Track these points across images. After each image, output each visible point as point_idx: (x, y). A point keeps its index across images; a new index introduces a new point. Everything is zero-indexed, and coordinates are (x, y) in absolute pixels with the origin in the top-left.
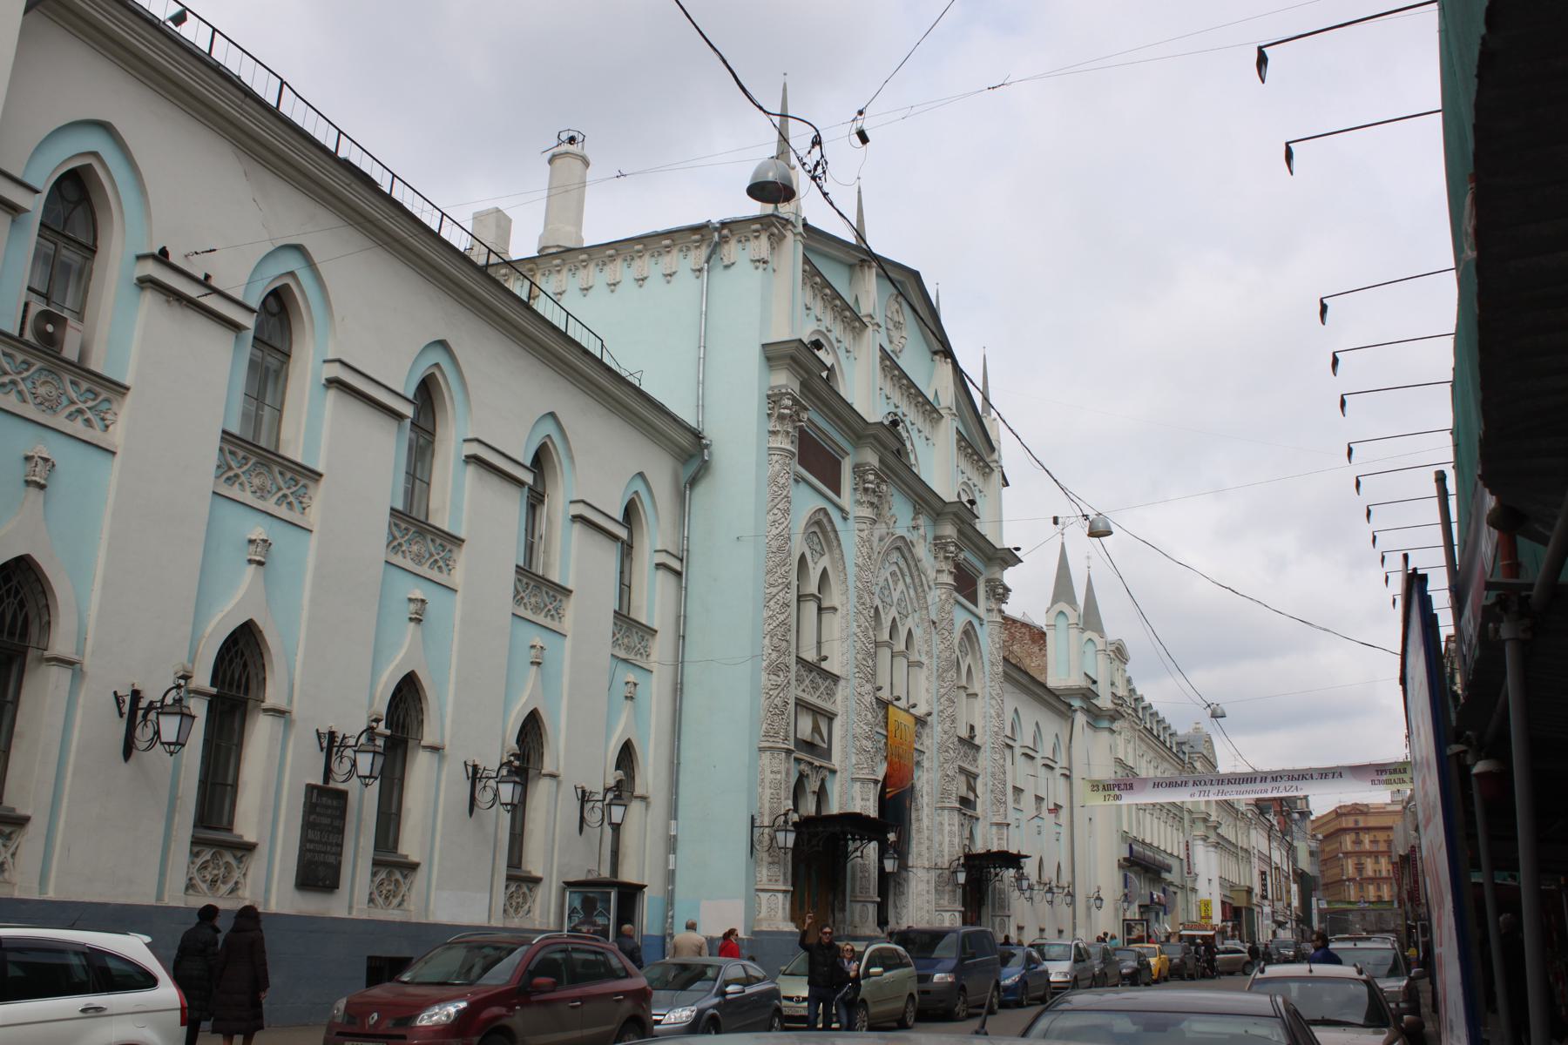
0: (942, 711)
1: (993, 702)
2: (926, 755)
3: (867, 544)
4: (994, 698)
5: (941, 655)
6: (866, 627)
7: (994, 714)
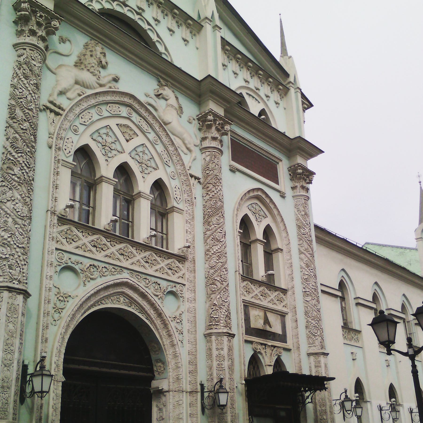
0: (208, 250)
1: (303, 256)
2: (187, 286)
3: (25, 66)
4: (302, 253)
5: (207, 204)
6: (15, 137)
7: (304, 266)
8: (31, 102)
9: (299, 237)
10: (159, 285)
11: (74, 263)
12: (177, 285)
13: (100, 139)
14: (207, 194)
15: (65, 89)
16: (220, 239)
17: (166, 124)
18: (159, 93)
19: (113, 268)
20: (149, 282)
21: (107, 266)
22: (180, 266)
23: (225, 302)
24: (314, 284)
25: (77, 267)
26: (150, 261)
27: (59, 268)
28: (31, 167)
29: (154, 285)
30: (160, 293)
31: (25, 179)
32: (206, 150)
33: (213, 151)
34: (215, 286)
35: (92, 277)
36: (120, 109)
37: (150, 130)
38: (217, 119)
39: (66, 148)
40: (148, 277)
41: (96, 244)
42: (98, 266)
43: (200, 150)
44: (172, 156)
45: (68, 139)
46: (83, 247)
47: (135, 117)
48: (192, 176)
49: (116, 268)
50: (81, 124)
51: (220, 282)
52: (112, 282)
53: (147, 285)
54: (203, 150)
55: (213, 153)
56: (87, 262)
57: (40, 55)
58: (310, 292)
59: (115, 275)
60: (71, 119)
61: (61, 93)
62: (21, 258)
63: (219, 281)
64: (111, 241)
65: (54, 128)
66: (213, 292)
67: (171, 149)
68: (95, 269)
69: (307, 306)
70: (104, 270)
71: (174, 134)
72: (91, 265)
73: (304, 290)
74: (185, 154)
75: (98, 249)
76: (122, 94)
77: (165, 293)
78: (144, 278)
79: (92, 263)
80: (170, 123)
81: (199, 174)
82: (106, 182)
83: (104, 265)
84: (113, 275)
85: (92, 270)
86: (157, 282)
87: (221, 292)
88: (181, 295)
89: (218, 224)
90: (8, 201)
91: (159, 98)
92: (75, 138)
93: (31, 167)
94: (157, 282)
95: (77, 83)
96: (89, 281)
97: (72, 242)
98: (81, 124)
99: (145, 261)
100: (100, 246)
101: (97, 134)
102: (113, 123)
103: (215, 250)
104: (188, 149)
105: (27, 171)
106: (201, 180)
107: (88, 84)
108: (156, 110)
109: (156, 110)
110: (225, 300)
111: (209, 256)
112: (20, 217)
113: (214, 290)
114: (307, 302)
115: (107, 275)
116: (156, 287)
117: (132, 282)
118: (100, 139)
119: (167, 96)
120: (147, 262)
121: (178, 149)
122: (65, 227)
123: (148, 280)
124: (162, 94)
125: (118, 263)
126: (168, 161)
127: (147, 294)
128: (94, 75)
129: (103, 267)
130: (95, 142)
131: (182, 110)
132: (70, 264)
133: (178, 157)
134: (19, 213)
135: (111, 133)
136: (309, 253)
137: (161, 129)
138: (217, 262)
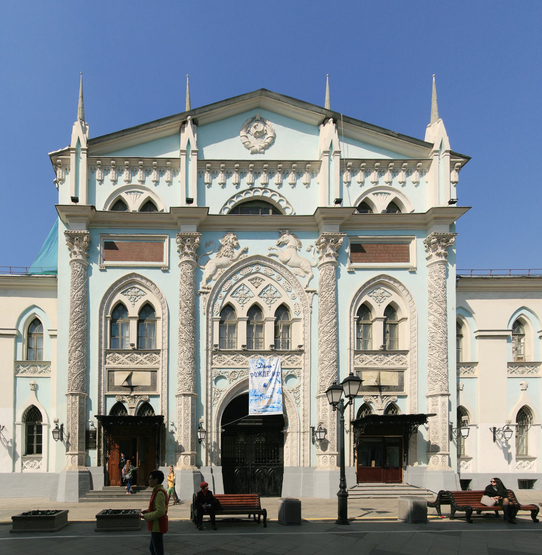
1: (431, 317)
7: (431, 325)
9: (430, 301)
14: (321, 300)
17: (285, 263)
24: (440, 339)
58: (435, 346)
67: (291, 278)
69: (431, 359)
73: (429, 346)
74: (303, 277)
80: (289, 261)
81: (317, 288)
90: (182, 352)
103: (324, 340)
106: (318, 292)
109: (277, 256)
111: (320, 345)
114: (431, 356)
119: (287, 241)
121: (297, 277)
131: (301, 245)
136: (438, 313)
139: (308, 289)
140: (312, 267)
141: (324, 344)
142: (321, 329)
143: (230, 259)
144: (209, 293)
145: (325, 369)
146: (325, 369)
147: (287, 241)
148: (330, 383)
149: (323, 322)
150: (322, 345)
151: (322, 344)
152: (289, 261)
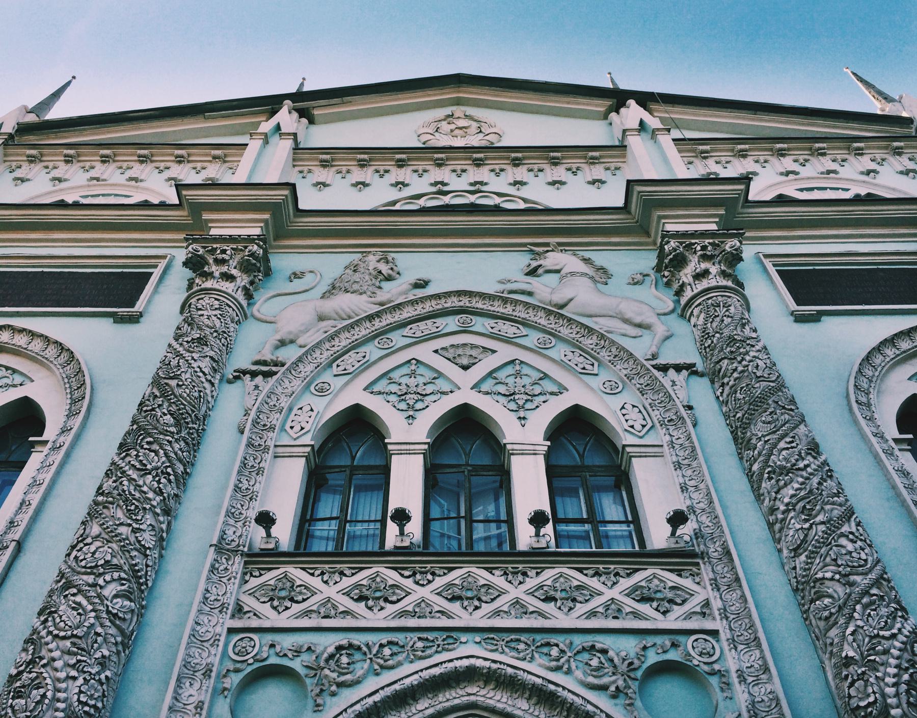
0: (773, 510)
2: (724, 635)
8: (180, 366)
10: (604, 652)
11: (285, 655)
12: (681, 639)
13: (394, 388)
15: (290, 333)
16: (795, 465)
17: (562, 307)
18: (534, 264)
19: (420, 639)
20: (562, 651)
21: (399, 637)
22: (687, 583)
23: (883, 637)
25: (296, 665)
26: (558, 595)
27: (235, 680)
28: (149, 467)
29: (585, 656)
30: (614, 678)
31: (124, 491)
32: (690, 307)
33: (708, 299)
34: (827, 601)
35: (342, 678)
36: (436, 325)
37: (524, 331)
38: (693, 241)
39: (292, 424)
40: (554, 639)
41: (366, 593)
42: (367, 645)
43: (682, 316)
44: (595, 354)
45: (301, 409)
46: (322, 610)
47: (480, 324)
48: (664, 369)
49: (430, 636)
50: (335, 376)
51: (838, 581)
52: (416, 677)
53: (554, 664)
54: (684, 313)
55: (710, 301)
56: (328, 643)
57: (216, 299)
59: (430, 656)
60: (307, 373)
61: (282, 343)
62: (59, 664)
63: (832, 579)
64: (414, 574)
65: (255, 398)
66: (830, 621)
67: (589, 342)
68: (358, 656)
70: (387, 651)
71: (590, 316)
72: (339, 648)
75: (370, 603)
76: (435, 299)
77: (639, 674)
78: (542, 645)
79: (344, 642)
80: (571, 300)
82: (401, 454)
83: (384, 638)
84: (421, 658)
85: (345, 660)
86: (593, 647)
87: (854, 610)
88: (706, 668)
89: (774, 432)
91: (538, 276)
92: (319, 403)
93: (149, 467)
94: (593, 647)
95: (321, 318)
96: (333, 694)
97: (288, 604)
98: (335, 376)
99: (543, 597)
100: (378, 594)
101: (384, 382)
102: (424, 352)
103: (786, 500)
104: (639, 326)
105: (135, 476)
106: (700, 367)
107: (348, 310)
108: (530, 294)
109: (530, 294)
110: (881, 633)
112: (84, 570)
113: (826, 614)
115: (400, 664)
116: (595, 663)
117: (487, 664)
118: (394, 388)
119: (557, 265)
120: (548, 599)
122: (270, 577)
123: (557, 645)
124: (541, 265)
125: (444, 622)
126: (590, 367)
127: (552, 687)
128: (361, 294)
129: (384, 641)
130: (381, 396)
132: (273, 660)
133: (614, 349)
134: (83, 563)
135: (421, 370)
137: (552, 318)
138: (807, 525)
139: (661, 361)
140: (658, 314)
141: (792, 514)
142: (755, 467)
143: (364, 297)
144: (275, 373)
145: (842, 621)
146: (842, 621)
147: (557, 265)
148: (904, 687)
149: (754, 441)
150: (784, 519)
151: (780, 516)
152: (571, 300)
